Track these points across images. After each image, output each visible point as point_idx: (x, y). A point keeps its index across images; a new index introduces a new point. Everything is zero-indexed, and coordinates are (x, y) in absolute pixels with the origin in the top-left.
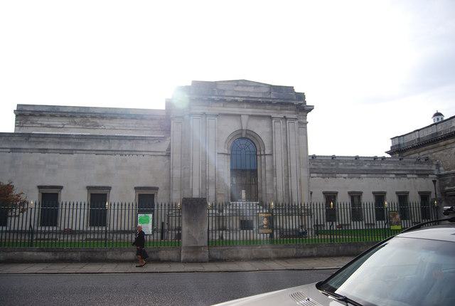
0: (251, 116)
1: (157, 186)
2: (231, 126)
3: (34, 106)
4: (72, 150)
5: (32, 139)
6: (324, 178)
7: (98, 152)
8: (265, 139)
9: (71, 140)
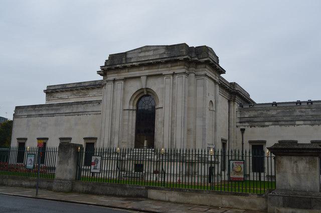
0: (148, 76)
1: (96, 137)
2: (134, 87)
3: (54, 86)
4: (54, 114)
5: (37, 109)
6: (312, 125)
7: (67, 114)
8: (159, 94)
9: (54, 107)
